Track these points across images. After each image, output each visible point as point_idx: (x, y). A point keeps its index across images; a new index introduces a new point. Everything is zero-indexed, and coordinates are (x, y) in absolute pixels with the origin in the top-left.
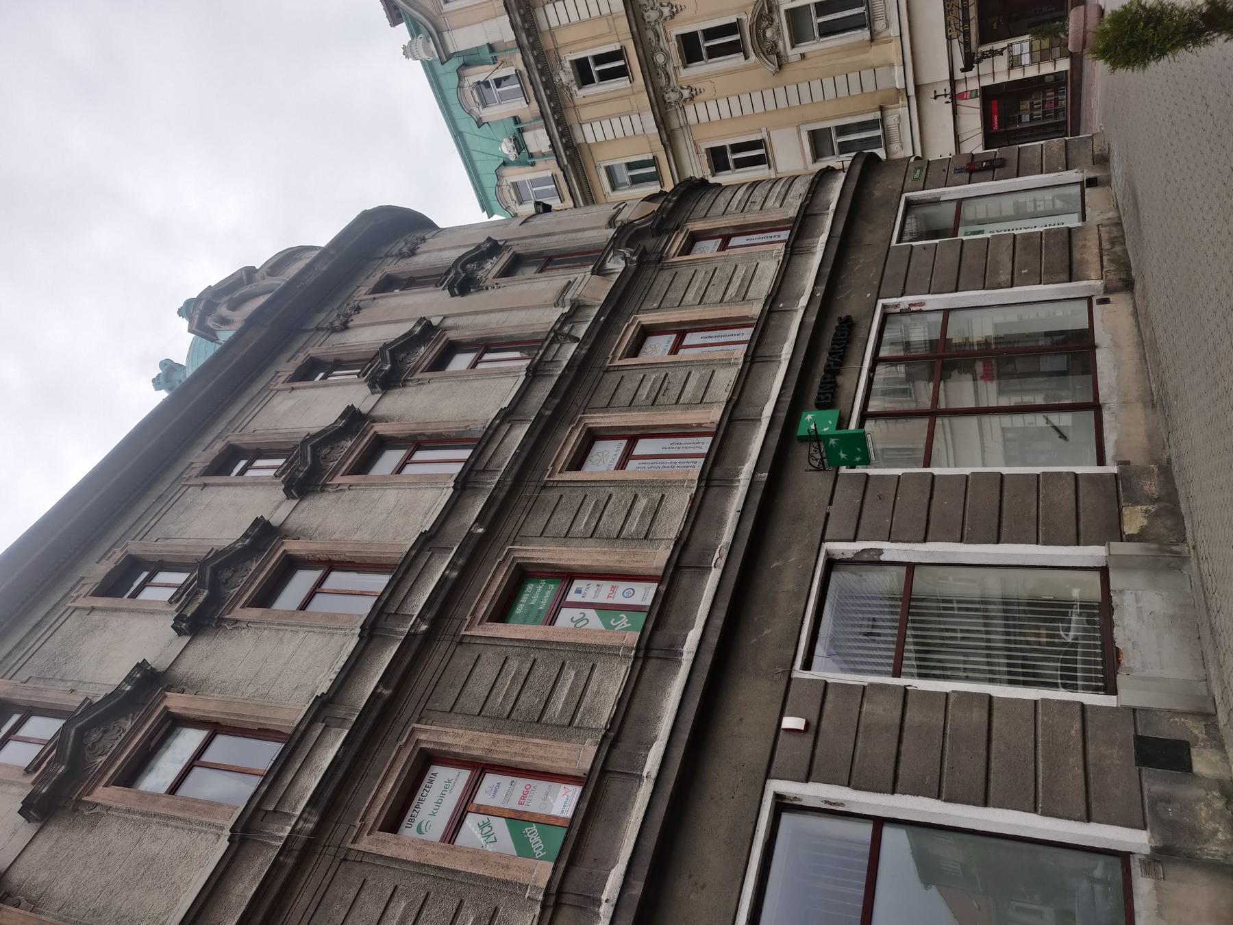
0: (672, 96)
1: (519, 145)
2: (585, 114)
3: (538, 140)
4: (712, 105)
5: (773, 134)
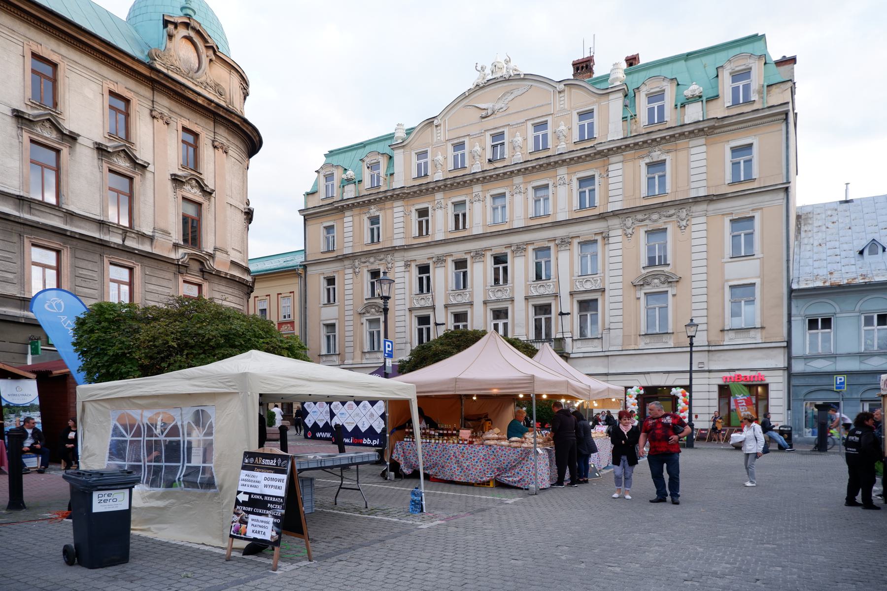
0: (357, 263)
1: (349, 181)
2: (357, 218)
3: (350, 192)
4: (619, 246)
5: (336, 308)
